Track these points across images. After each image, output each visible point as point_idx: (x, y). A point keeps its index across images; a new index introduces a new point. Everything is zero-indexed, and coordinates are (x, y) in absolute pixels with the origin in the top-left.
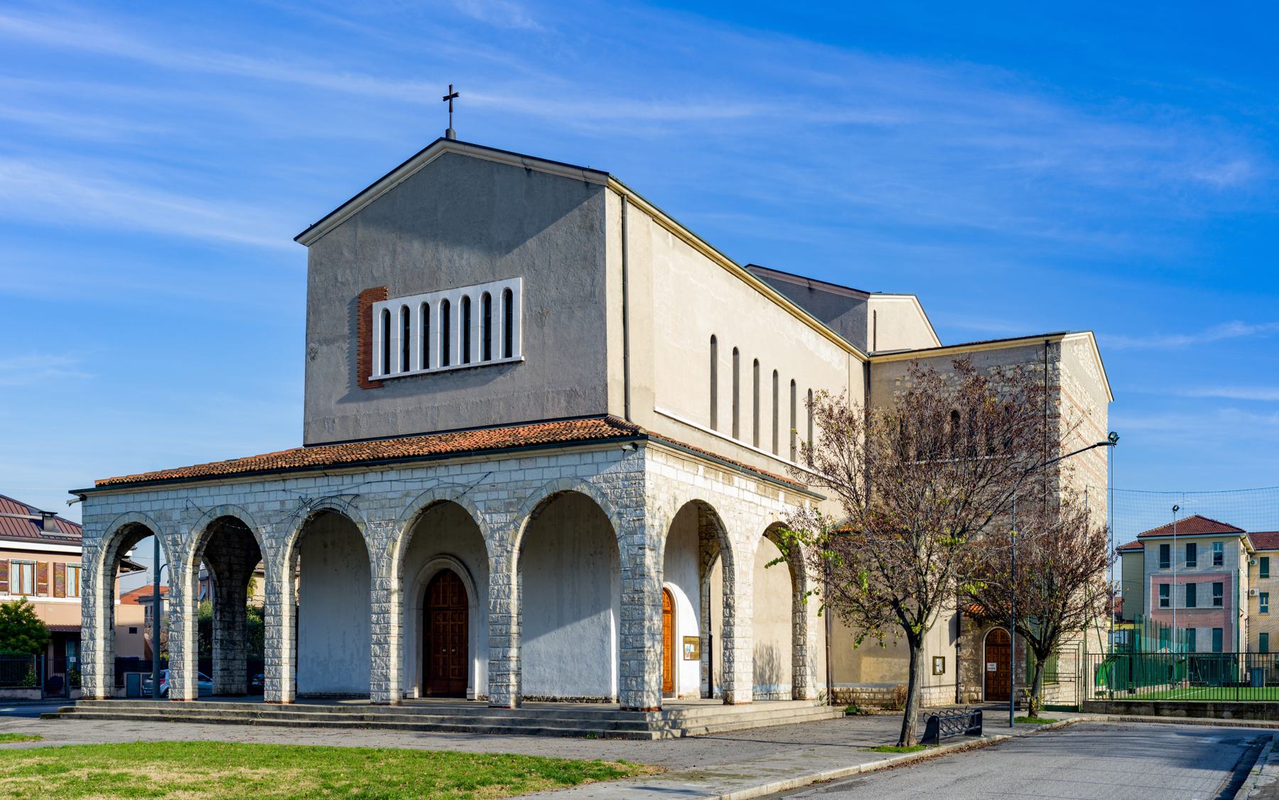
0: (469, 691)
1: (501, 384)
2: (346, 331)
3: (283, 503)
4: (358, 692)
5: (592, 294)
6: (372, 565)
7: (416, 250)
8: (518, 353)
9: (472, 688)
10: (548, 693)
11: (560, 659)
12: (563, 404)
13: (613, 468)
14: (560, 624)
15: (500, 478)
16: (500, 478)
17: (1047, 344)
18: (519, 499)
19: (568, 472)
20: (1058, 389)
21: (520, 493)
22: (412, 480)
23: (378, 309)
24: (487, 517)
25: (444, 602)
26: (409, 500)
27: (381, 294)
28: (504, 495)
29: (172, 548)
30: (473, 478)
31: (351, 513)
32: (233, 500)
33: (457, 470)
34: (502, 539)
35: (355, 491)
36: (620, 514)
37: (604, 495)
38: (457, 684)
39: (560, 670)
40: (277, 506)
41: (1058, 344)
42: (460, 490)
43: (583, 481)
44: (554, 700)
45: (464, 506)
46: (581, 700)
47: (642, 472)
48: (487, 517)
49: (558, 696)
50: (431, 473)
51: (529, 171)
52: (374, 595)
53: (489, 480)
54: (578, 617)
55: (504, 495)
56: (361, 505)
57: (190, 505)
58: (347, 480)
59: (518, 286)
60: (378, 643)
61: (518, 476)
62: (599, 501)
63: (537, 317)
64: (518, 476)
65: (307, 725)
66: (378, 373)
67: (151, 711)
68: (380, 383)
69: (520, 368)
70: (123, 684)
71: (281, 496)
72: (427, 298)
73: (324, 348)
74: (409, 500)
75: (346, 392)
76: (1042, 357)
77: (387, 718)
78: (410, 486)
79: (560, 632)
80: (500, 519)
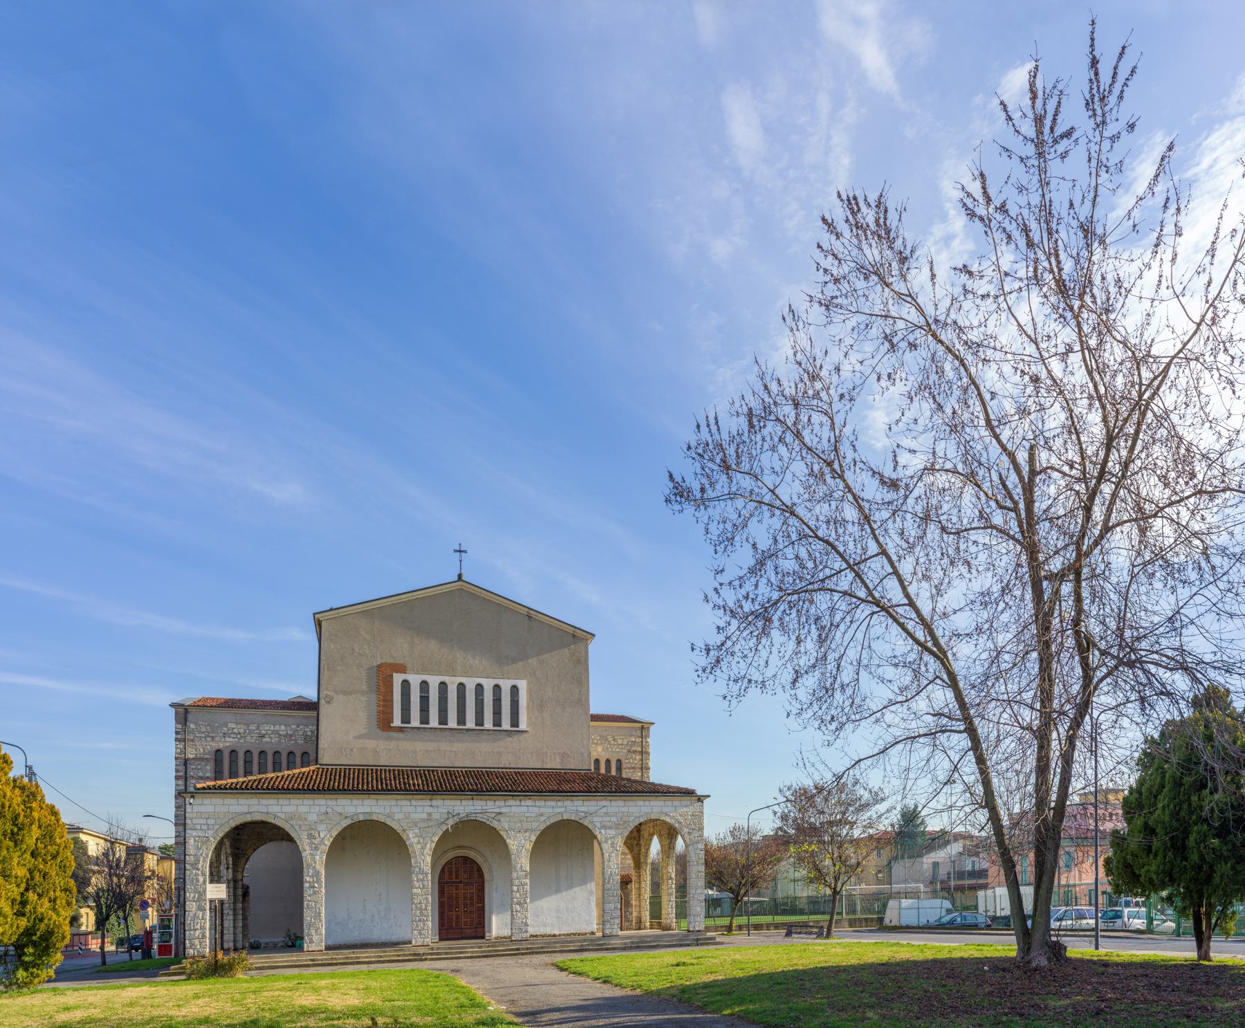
0: (487, 934)
1: (509, 742)
2: (364, 687)
3: (430, 814)
4: (380, 941)
5: (580, 700)
6: (513, 857)
7: (433, 647)
8: (523, 725)
9: (490, 931)
10: (548, 931)
11: (558, 911)
12: (558, 760)
13: (685, 809)
14: (558, 891)
15: (611, 810)
16: (611, 810)
17: (643, 727)
18: (625, 822)
19: (656, 810)
20: (648, 754)
21: (625, 819)
22: (545, 806)
23: (398, 679)
24: (603, 831)
25: (457, 878)
26: (542, 819)
27: (402, 669)
28: (614, 819)
29: (308, 841)
30: (592, 809)
31: (495, 824)
32: (375, 809)
33: (580, 803)
34: (613, 843)
35: (498, 810)
36: (689, 833)
37: (680, 823)
38: (478, 929)
39: (558, 918)
40: (425, 816)
41: (648, 728)
42: (583, 814)
43: (666, 815)
44: (555, 936)
45: (586, 824)
46: (574, 934)
47: (702, 813)
48: (603, 831)
49: (557, 933)
50: (560, 804)
51: (530, 617)
52: (515, 875)
53: (604, 810)
54: (570, 887)
55: (614, 819)
56: (502, 819)
57: (329, 810)
58: (490, 803)
59: (523, 685)
60: (519, 904)
61: (625, 809)
62: (677, 826)
63: (538, 704)
64: (625, 809)
65: (468, 958)
66: (397, 722)
67: (370, 957)
68: (400, 729)
69: (525, 735)
70: (171, 951)
71: (430, 810)
72: (446, 679)
73: (341, 697)
74: (542, 819)
75: (365, 731)
76: (639, 734)
77: (456, 953)
78: (542, 810)
79: (559, 896)
80: (611, 832)
